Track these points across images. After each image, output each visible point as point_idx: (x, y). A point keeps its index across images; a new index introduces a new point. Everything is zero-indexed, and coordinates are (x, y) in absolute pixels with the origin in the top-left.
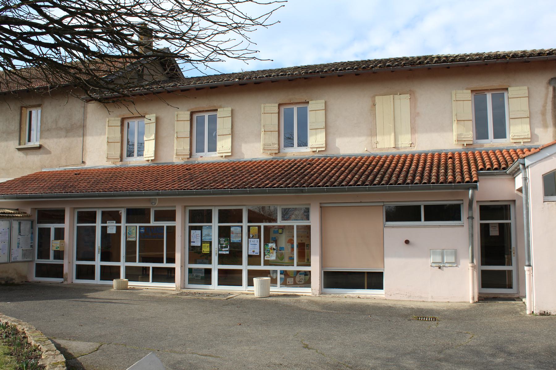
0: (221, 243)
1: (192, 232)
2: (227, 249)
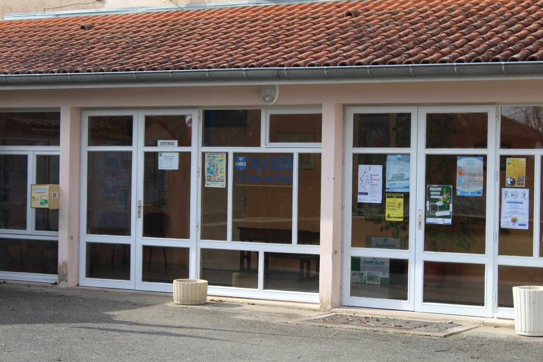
0: (432, 197)
1: (362, 168)
2: (447, 213)
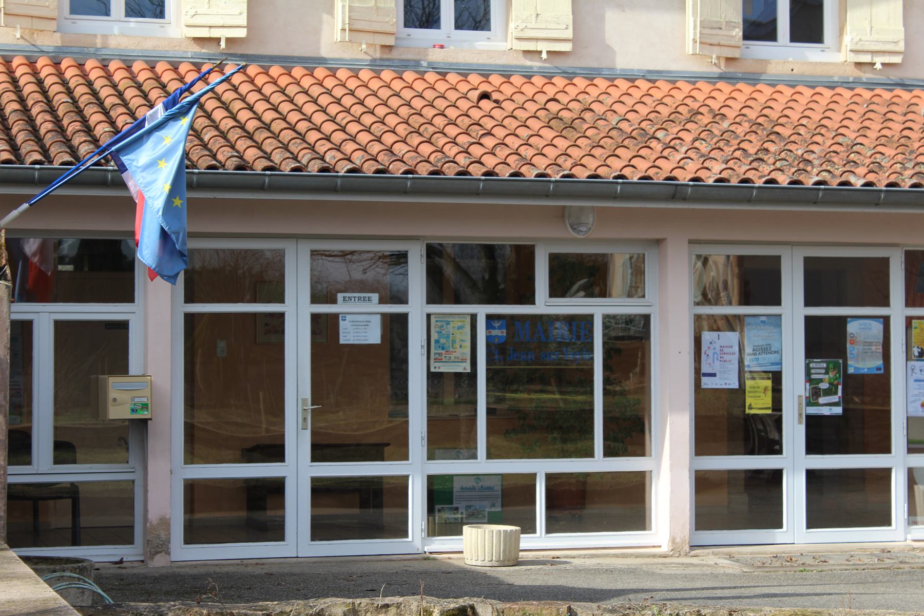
0: (813, 377)
2: (835, 399)
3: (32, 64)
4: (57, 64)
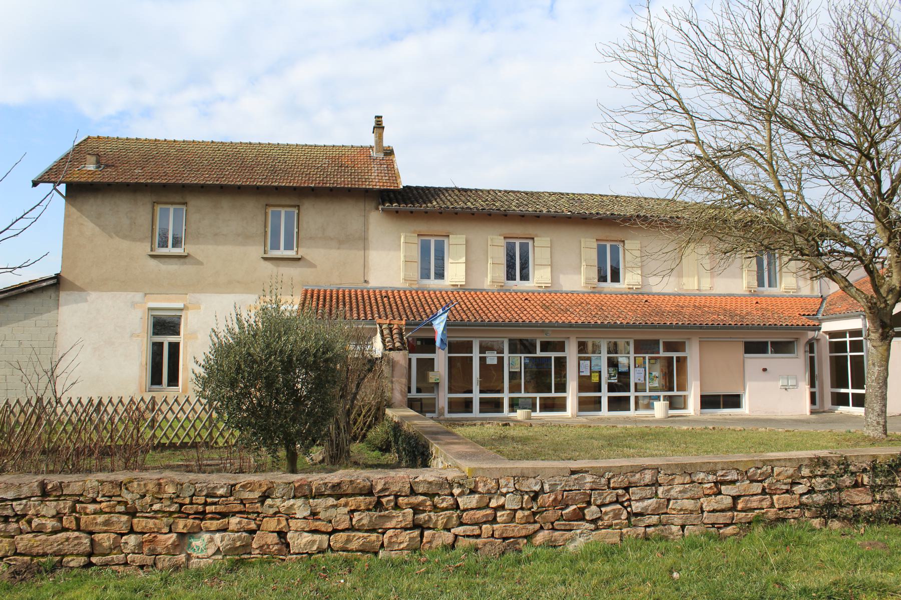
1: (581, 362)
3: (411, 292)
4: (417, 292)
